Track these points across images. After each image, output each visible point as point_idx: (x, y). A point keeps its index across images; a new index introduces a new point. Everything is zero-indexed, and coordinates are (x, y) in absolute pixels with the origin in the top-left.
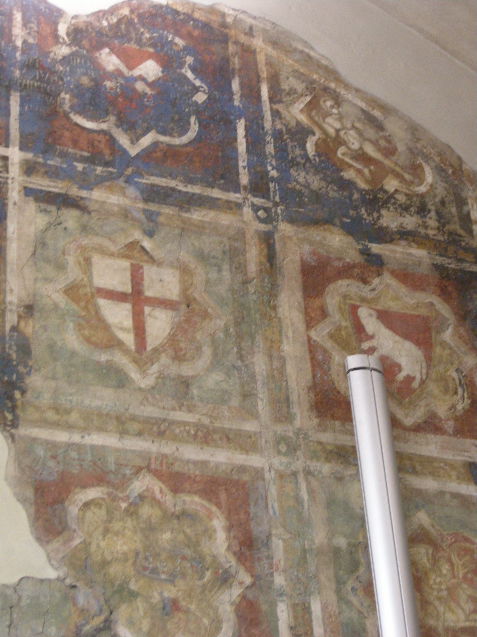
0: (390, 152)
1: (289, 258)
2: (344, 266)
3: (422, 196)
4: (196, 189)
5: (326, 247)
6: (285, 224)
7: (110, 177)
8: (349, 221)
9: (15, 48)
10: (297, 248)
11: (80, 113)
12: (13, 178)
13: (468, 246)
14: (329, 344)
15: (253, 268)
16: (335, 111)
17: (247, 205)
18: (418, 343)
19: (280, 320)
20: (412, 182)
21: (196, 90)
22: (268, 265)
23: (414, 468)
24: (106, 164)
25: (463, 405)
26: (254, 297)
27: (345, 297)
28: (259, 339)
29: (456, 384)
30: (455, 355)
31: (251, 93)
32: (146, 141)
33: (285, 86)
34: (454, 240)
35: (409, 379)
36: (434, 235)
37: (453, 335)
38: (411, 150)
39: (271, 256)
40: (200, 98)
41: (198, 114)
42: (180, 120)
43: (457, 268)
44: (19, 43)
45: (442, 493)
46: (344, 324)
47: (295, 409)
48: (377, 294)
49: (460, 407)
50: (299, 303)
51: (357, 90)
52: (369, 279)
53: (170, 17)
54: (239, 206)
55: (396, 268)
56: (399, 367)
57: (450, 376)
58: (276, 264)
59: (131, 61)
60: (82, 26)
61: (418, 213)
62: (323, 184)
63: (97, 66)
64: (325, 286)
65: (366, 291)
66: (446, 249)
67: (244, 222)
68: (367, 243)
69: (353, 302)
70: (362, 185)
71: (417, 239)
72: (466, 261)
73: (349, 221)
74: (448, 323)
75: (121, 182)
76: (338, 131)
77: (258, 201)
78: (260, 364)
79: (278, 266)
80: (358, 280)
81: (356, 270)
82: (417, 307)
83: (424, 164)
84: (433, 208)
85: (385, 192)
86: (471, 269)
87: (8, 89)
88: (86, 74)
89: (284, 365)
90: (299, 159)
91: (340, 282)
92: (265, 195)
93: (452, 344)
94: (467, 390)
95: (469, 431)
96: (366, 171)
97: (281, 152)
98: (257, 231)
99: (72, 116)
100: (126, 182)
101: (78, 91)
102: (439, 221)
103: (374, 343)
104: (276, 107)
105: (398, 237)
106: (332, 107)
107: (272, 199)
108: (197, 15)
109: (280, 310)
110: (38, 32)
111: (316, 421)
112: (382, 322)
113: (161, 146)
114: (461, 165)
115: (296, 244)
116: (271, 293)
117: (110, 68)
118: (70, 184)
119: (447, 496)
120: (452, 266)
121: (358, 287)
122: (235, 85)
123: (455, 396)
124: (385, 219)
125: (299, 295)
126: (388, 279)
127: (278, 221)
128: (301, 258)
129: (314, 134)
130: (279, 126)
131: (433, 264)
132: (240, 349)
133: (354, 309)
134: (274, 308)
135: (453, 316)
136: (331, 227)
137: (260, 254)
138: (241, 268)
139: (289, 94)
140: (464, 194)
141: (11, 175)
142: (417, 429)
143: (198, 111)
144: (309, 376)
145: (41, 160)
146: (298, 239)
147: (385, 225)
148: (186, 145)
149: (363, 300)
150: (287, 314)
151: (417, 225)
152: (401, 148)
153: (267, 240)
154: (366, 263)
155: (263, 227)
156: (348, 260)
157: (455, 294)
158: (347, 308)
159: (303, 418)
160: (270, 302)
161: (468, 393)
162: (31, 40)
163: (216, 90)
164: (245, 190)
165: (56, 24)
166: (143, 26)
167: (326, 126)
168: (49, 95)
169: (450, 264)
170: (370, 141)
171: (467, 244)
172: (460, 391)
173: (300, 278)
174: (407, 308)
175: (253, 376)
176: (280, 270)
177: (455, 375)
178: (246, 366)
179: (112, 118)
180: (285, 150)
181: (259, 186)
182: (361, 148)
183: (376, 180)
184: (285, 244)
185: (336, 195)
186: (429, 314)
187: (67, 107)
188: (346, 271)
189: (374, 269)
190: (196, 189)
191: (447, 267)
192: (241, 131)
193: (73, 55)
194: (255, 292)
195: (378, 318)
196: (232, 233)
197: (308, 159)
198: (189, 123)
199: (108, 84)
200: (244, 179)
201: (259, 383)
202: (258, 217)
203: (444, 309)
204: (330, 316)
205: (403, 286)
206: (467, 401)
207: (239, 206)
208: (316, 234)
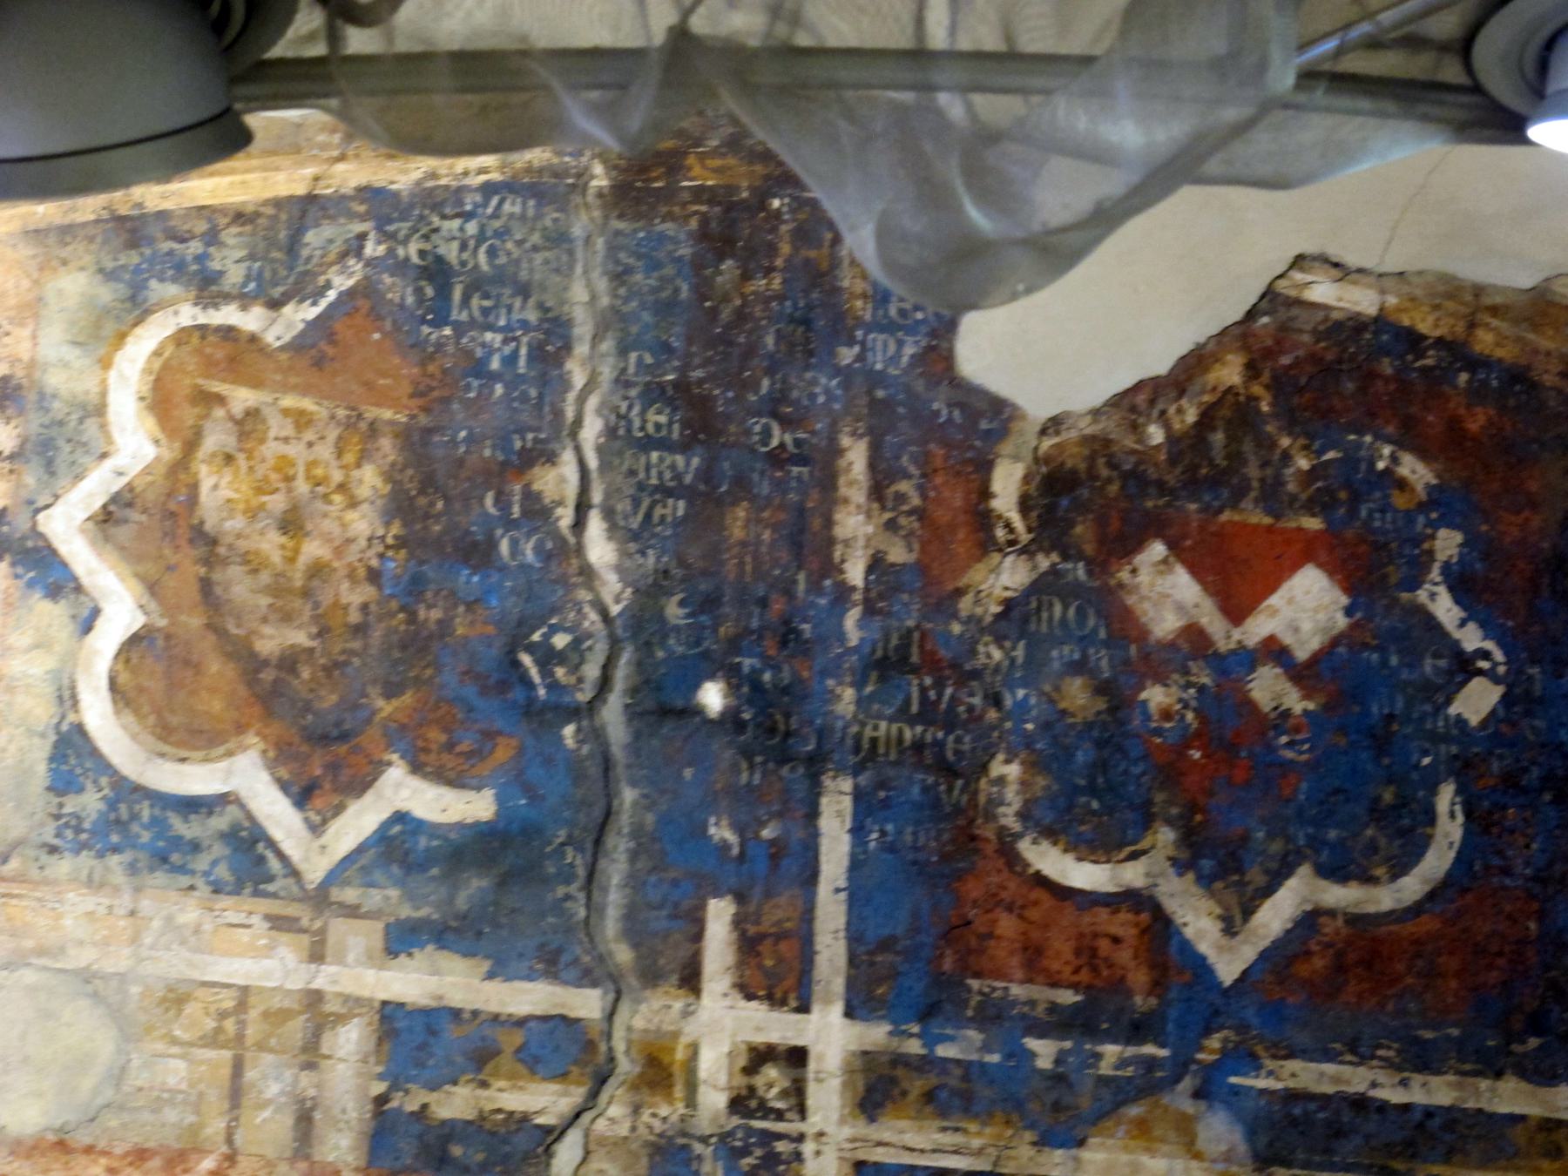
4: (1436, 1091)
7: (1147, 1083)
9: (843, 593)
11: (1050, 833)
12: (821, 1134)
21: (1464, 667)
24: (1137, 1031)
32: (1276, 915)
40: (1476, 701)
41: (1464, 769)
42: (1402, 804)
44: (856, 573)
53: (1387, 367)
59: (1238, 581)
60: (1074, 460)
63: (1122, 626)
75: (1181, 1099)
87: (816, 765)
88: (1079, 667)
99: (1026, 847)
100: (1198, 1095)
101: (1049, 750)
108: (1485, 341)
110: (920, 513)
113: (1329, 927)
117: (1165, 625)
118: (1010, 1132)
141: (815, 1121)
143: (1466, 757)
145: (914, 1047)
148: (1416, 910)
162: (898, 554)
163: (1533, 662)
165: (985, 467)
166: (1291, 420)
168: (949, 771)
179: (1165, 837)
187: (1008, 817)
190: (1436, 1091)
193: (1041, 587)
198: (1431, 817)
199: (1156, 696)
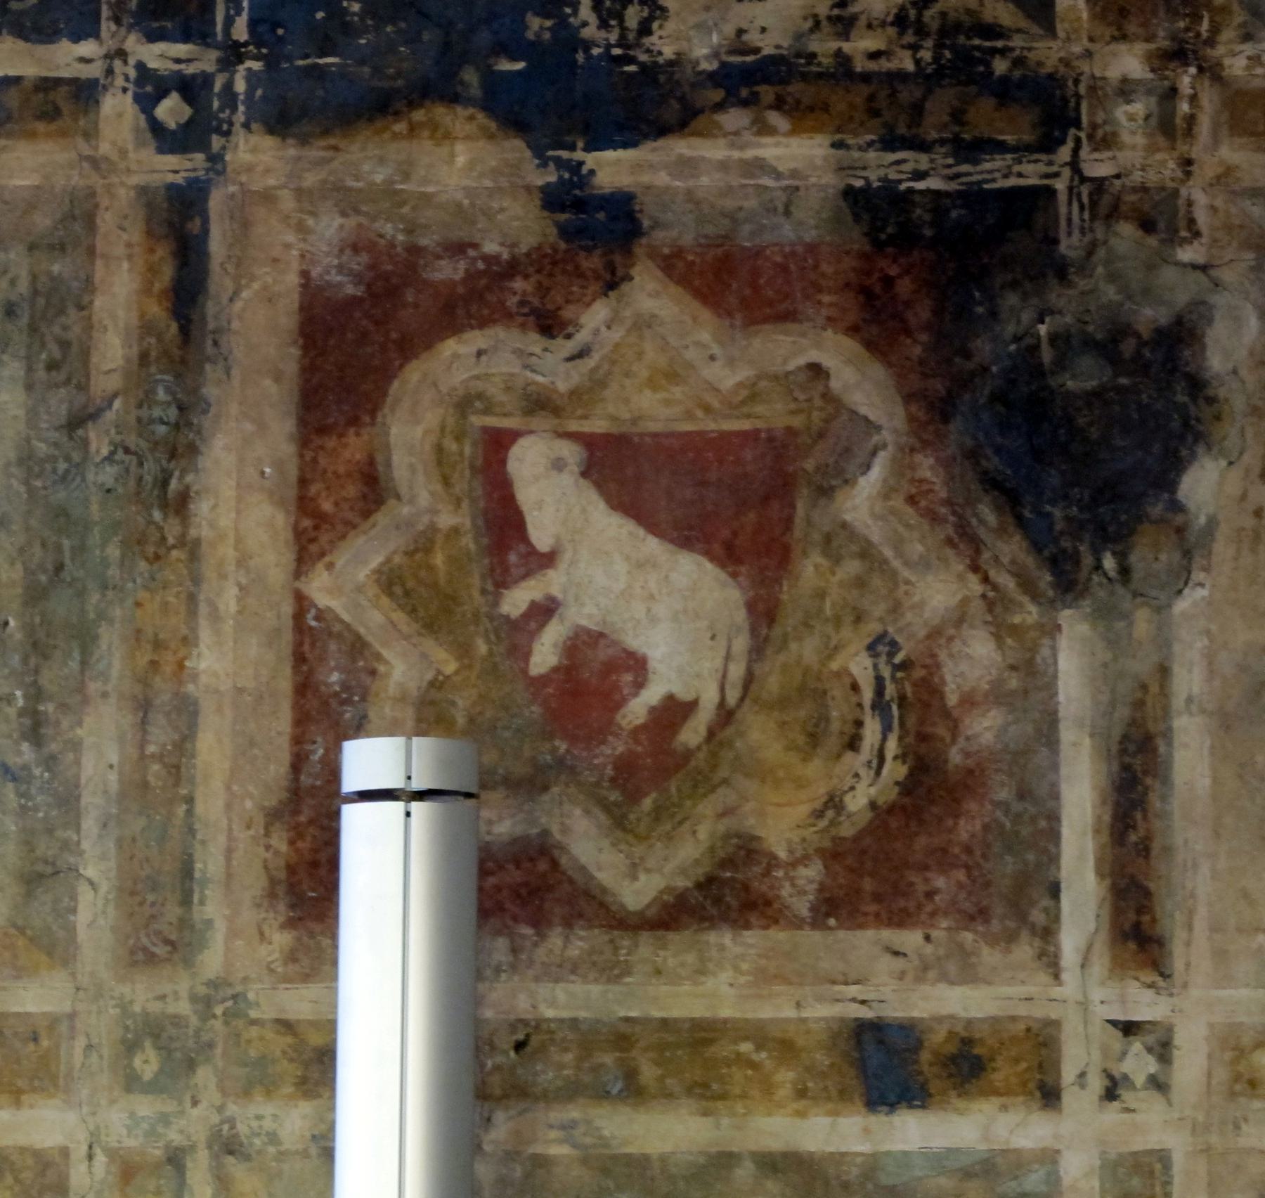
1: (256, 286)
2: (470, 276)
5: (405, 210)
6: (254, 139)
8: (520, 65)
10: (290, 238)
13: (1017, 74)
14: (374, 618)
15: (112, 352)
17: (120, 82)
18: (728, 556)
19: (193, 550)
22: (174, 327)
23: (631, 1075)
25: (873, 791)
26: (108, 475)
27: (465, 403)
28: (111, 641)
29: (860, 705)
30: (877, 581)
35: (674, 711)
36: (874, 56)
37: (886, 494)
39: (186, 292)
43: (953, 186)
45: (724, 1161)
46: (446, 520)
47: (212, 908)
48: (594, 370)
49: (857, 802)
50: (279, 465)
52: (568, 313)
54: (85, 93)
55: (688, 239)
56: (638, 666)
57: (844, 672)
58: (203, 319)
64: (385, 375)
65: (552, 367)
66: (917, 111)
67: (95, 162)
68: (579, 155)
69: (492, 421)
71: (795, 88)
72: (1002, 147)
73: (520, 65)
74: (876, 439)
77: (159, 55)
78: (101, 747)
79: (211, 325)
80: (523, 326)
81: (518, 284)
82: (753, 397)
86: (1012, 182)
89: (184, 743)
91: (450, 347)
93: (875, 533)
94: (902, 724)
95: (877, 898)
98: (143, 190)
103: (553, 582)
105: (717, 95)
107: (220, 37)
109: (202, 508)
111: (282, 939)
112: (599, 486)
115: (291, 215)
116: (179, 443)
119: (744, 1173)
120: (933, 183)
121: (519, 353)
123: (849, 756)
124: (671, 26)
125: (281, 430)
126: (649, 293)
127: (227, 134)
128: (305, 274)
131: (849, 193)
132: (36, 694)
133: (498, 444)
134: (181, 505)
135: (900, 411)
136: (440, 112)
137: (146, 290)
138: (65, 363)
142: (672, 915)
144: (277, 770)
146: (300, 193)
147: (668, 52)
149: (540, 404)
150: (226, 521)
151: (809, 24)
154: (563, 246)
155: (172, 168)
156: (490, 247)
157: (922, 312)
158: (468, 450)
159: (234, 932)
160: (165, 483)
161: (900, 739)
164: (117, 20)
169: (919, 175)
171: (1019, 62)
172: (871, 730)
173: (290, 360)
174: (707, 409)
175: (69, 802)
176: (216, 343)
177: (861, 667)
178: (50, 762)
184: (246, 225)
186: (797, 422)
189: (592, 262)
191: (911, 191)
194: (110, 459)
195: (585, 474)
196: (43, 221)
201: (90, 824)
202: (156, 128)
203: (864, 387)
204: (398, 497)
205: (706, 314)
206: (895, 770)
207: (85, 93)
208: (370, 159)
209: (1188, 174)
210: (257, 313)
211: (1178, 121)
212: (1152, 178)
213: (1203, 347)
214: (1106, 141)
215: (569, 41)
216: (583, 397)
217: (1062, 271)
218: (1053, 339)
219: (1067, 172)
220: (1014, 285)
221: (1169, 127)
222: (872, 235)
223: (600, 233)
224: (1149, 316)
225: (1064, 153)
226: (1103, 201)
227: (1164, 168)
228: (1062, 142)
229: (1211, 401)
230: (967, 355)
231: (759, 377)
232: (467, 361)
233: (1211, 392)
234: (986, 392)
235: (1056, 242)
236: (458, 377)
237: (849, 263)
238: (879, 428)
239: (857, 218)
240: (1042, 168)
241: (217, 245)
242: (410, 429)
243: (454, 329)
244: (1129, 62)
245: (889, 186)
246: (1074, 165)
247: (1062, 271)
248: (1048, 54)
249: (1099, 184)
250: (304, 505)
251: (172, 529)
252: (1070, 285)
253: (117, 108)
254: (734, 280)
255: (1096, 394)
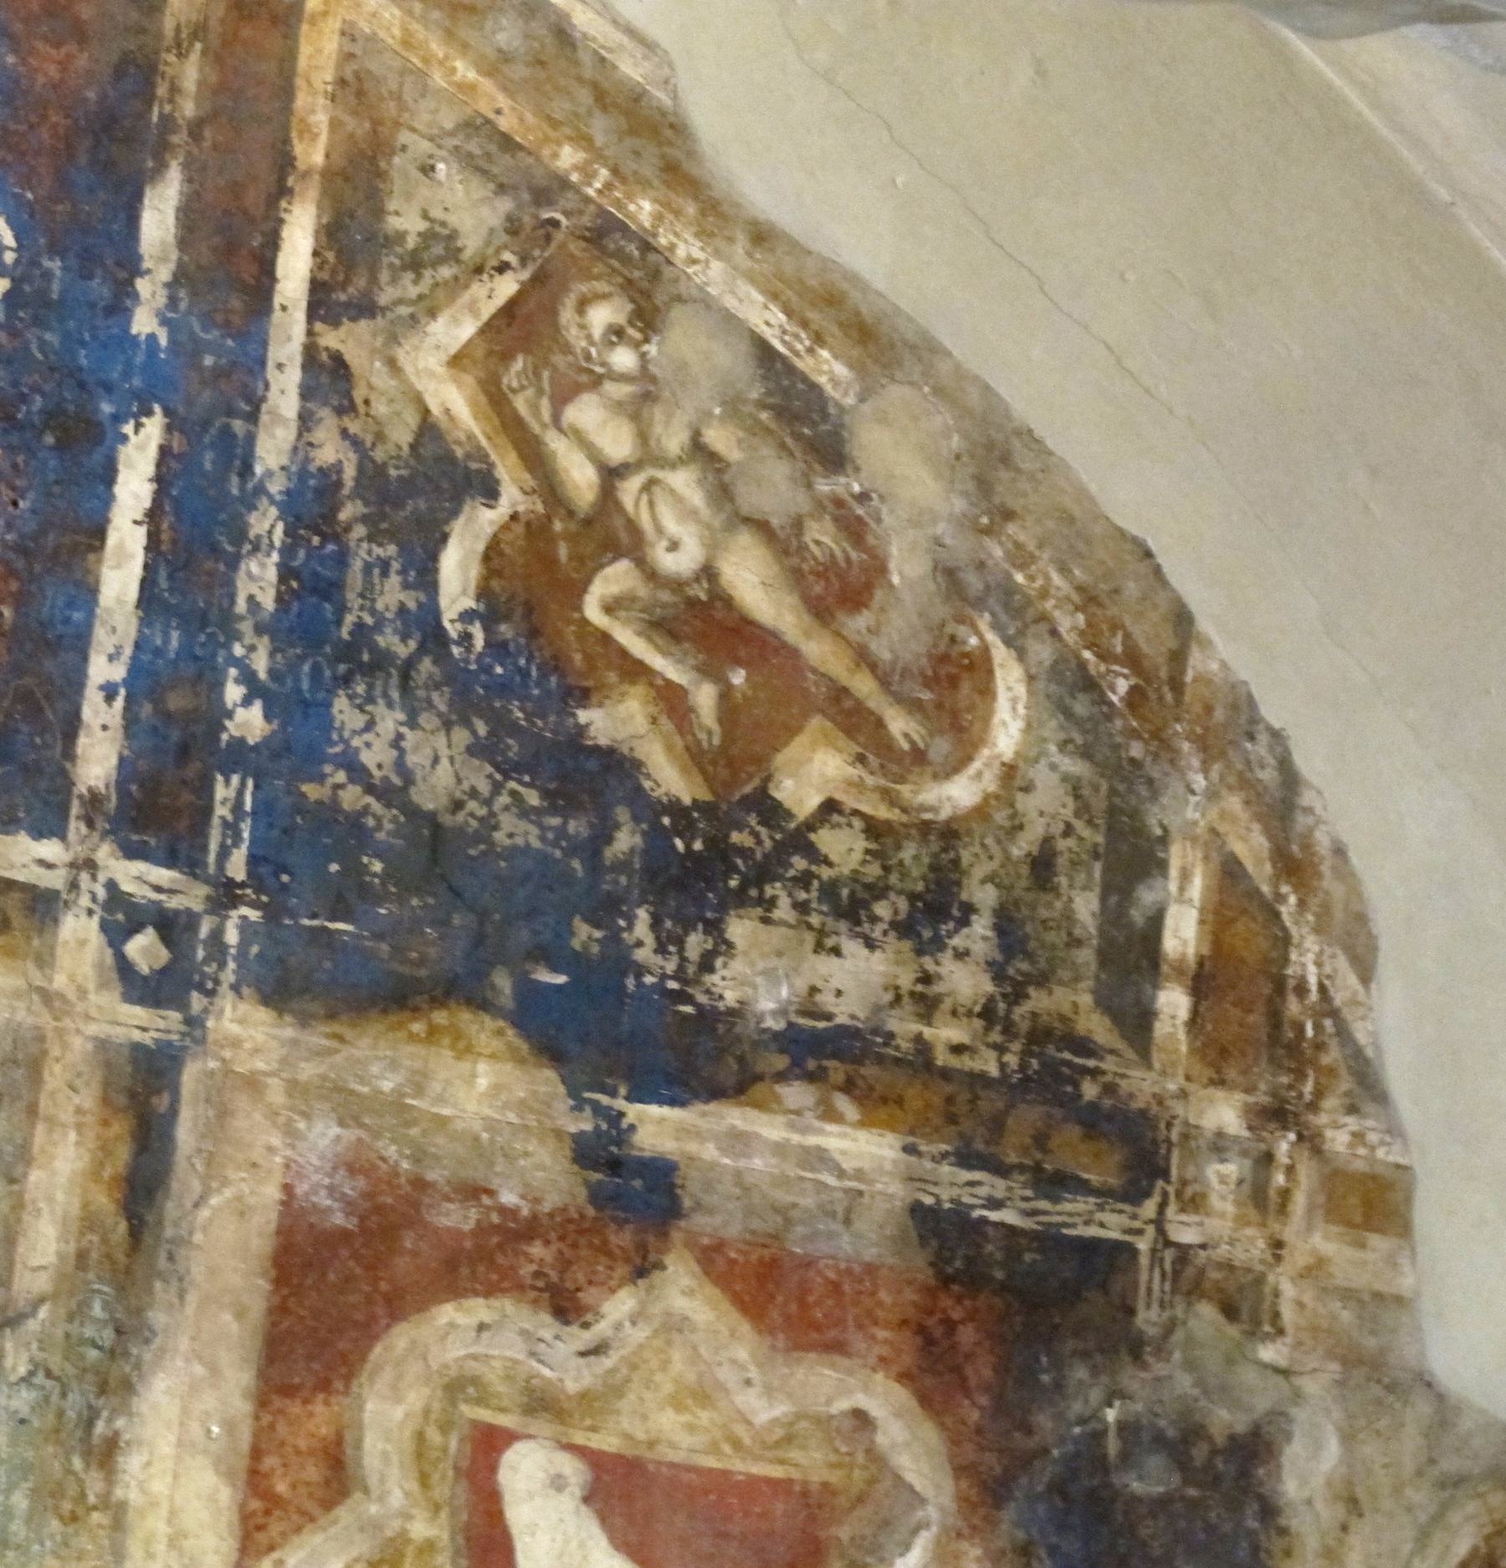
0: (840, 590)
1: (228, 1193)
2: (481, 1230)
3: (950, 833)
5: (414, 1132)
6: (243, 1007)
8: (561, 979)
10: (276, 1141)
13: (1107, 1102)
16: (623, 359)
17: (85, 901)
19: (118, 1515)
20: (919, 756)
22: (123, 1226)
27: (457, 1387)
31: (232, 262)
33: (405, 221)
34: (1051, 1068)
36: (957, 1049)
38: (949, 575)
39: (141, 1186)
46: (420, 1529)
48: (612, 1371)
50: (229, 1426)
51: (762, 236)
52: (587, 1296)
54: (43, 906)
55: (733, 1231)
58: (160, 1223)
61: (903, 928)
62: (479, 776)
64: (369, 1332)
65: (562, 1361)
66: (997, 1126)
67: (47, 997)
68: (620, 1104)
69: (485, 1415)
70: (670, 778)
71: (869, 1071)
72: (1085, 1188)
73: (561, 979)
76: (611, 474)
77: (138, 877)
79: (169, 1232)
80: (535, 1302)
81: (536, 1250)
82: (789, 1440)
83: (1000, 653)
84: (985, 897)
85: (770, 810)
86: (1092, 1231)
90: (388, 640)
91: (447, 1313)
92: (182, 851)
96: (705, 698)
97: (311, 588)
98: (102, 1044)
102: (997, 972)
104: (330, 339)
105: (781, 1062)
106: (616, 333)
107: (212, 869)
109: (132, 1464)
112: (604, 1520)
114: (1178, 658)
121: (524, 1333)
122: (158, 221)
124: (738, 966)
125: (237, 1380)
126: (683, 1290)
127: (210, 994)
128: (287, 1189)
129: (490, 492)
130: (329, 451)
131: (916, 1209)
133: (489, 1444)
134: (106, 1455)
135: (948, 1484)
136: (465, 1017)
137: (95, 1173)
139: (415, 264)
140: (1153, 819)
146: (294, 1087)
147: (731, 997)
149: (542, 1403)
150: (159, 1486)
151: (888, 997)
152: (906, 566)
153: (142, 1092)
154: (591, 1212)
155: (138, 1023)
156: (508, 1198)
157: (982, 1370)
158: (453, 1444)
160: (90, 1424)
163: (54, 250)
164: (90, 824)
167: (558, 446)
169: (995, 1204)
170: (761, 527)
171: (1110, 1089)
173: (257, 1293)
174: (737, 1444)
176: (171, 1258)
180: (329, 590)
181: (157, 812)
182: (708, 572)
183: (737, 764)
184: (224, 1113)
185: (529, 835)
186: (835, 1477)
188: (487, 1259)
189: (621, 1239)
191: (984, 1221)
192: (134, 488)
194: (26, 1380)
195: (586, 1500)
197: (433, 636)
200: (97, 760)
202: (124, 968)
203: (913, 1449)
204: (366, 1491)
205: (745, 1328)
207: (43, 906)
208: (380, 1059)
209: (1278, 1258)
210: (225, 1225)
211: (1272, 1193)
212: (1239, 1256)
213: (1279, 1467)
214: (1194, 1203)
215: (619, 960)
216: (596, 1404)
217: (1136, 1348)
218: (1122, 1426)
219: (1151, 1231)
220: (1085, 1355)
221: (1262, 1199)
222: (938, 1264)
223: (633, 1205)
224: (1224, 1420)
225: (1149, 1208)
226: (1186, 1272)
227: (1251, 1248)
228: (1148, 1194)
229: (1283, 1532)
230: (1029, 1431)
231: (799, 1416)
232: (467, 1336)
233: (1282, 1522)
234: (1046, 1479)
235: (1131, 1312)
236: (455, 1351)
237: (910, 1295)
238: (923, 1501)
239: (923, 1241)
240: (1124, 1220)
241: (185, 1134)
242: (388, 1410)
243: (455, 1292)
244: (1224, 1113)
245: (960, 1213)
246: (1159, 1222)
247: (1136, 1348)
248: (1141, 1085)
249: (1184, 1253)
250: (255, 1480)
251: (94, 1484)
252: (1144, 1366)
253: (79, 931)
254: (778, 1291)
255: (1162, 1504)
